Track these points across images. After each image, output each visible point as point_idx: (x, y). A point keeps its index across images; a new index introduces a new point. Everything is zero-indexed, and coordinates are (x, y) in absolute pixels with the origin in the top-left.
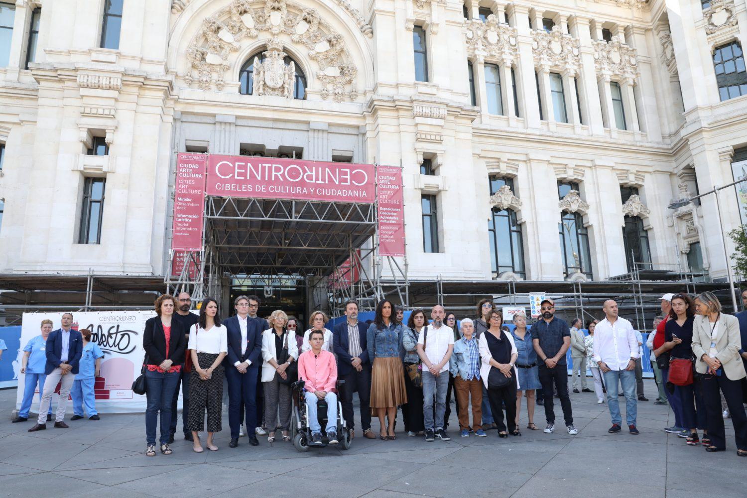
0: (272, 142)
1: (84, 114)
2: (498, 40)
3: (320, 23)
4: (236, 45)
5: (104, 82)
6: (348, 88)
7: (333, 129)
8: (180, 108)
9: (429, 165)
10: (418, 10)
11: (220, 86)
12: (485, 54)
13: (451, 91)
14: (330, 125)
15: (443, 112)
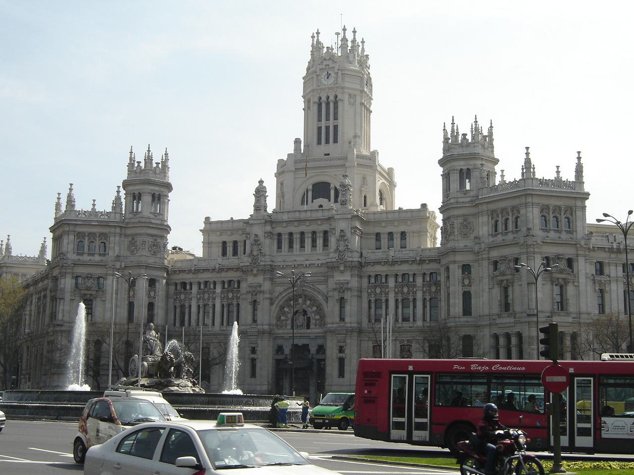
0: (300, 342)
1: (250, 344)
2: (381, 291)
3: (314, 300)
4: (289, 312)
5: (253, 334)
6: (323, 322)
7: (317, 337)
8: (275, 335)
9: (341, 350)
10: (341, 294)
11: (286, 327)
12: (374, 299)
13: (351, 323)
14: (316, 336)
15: (344, 333)
